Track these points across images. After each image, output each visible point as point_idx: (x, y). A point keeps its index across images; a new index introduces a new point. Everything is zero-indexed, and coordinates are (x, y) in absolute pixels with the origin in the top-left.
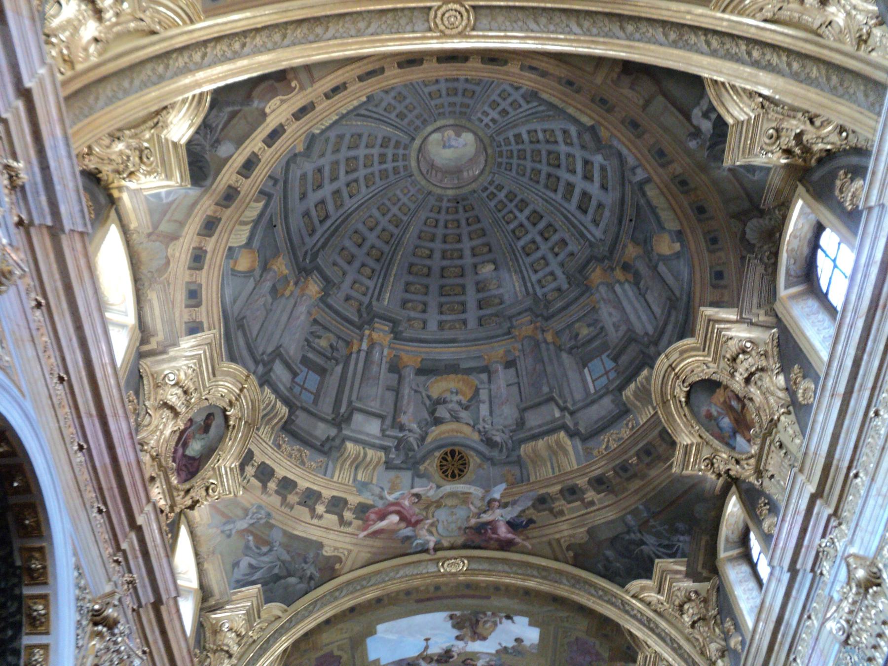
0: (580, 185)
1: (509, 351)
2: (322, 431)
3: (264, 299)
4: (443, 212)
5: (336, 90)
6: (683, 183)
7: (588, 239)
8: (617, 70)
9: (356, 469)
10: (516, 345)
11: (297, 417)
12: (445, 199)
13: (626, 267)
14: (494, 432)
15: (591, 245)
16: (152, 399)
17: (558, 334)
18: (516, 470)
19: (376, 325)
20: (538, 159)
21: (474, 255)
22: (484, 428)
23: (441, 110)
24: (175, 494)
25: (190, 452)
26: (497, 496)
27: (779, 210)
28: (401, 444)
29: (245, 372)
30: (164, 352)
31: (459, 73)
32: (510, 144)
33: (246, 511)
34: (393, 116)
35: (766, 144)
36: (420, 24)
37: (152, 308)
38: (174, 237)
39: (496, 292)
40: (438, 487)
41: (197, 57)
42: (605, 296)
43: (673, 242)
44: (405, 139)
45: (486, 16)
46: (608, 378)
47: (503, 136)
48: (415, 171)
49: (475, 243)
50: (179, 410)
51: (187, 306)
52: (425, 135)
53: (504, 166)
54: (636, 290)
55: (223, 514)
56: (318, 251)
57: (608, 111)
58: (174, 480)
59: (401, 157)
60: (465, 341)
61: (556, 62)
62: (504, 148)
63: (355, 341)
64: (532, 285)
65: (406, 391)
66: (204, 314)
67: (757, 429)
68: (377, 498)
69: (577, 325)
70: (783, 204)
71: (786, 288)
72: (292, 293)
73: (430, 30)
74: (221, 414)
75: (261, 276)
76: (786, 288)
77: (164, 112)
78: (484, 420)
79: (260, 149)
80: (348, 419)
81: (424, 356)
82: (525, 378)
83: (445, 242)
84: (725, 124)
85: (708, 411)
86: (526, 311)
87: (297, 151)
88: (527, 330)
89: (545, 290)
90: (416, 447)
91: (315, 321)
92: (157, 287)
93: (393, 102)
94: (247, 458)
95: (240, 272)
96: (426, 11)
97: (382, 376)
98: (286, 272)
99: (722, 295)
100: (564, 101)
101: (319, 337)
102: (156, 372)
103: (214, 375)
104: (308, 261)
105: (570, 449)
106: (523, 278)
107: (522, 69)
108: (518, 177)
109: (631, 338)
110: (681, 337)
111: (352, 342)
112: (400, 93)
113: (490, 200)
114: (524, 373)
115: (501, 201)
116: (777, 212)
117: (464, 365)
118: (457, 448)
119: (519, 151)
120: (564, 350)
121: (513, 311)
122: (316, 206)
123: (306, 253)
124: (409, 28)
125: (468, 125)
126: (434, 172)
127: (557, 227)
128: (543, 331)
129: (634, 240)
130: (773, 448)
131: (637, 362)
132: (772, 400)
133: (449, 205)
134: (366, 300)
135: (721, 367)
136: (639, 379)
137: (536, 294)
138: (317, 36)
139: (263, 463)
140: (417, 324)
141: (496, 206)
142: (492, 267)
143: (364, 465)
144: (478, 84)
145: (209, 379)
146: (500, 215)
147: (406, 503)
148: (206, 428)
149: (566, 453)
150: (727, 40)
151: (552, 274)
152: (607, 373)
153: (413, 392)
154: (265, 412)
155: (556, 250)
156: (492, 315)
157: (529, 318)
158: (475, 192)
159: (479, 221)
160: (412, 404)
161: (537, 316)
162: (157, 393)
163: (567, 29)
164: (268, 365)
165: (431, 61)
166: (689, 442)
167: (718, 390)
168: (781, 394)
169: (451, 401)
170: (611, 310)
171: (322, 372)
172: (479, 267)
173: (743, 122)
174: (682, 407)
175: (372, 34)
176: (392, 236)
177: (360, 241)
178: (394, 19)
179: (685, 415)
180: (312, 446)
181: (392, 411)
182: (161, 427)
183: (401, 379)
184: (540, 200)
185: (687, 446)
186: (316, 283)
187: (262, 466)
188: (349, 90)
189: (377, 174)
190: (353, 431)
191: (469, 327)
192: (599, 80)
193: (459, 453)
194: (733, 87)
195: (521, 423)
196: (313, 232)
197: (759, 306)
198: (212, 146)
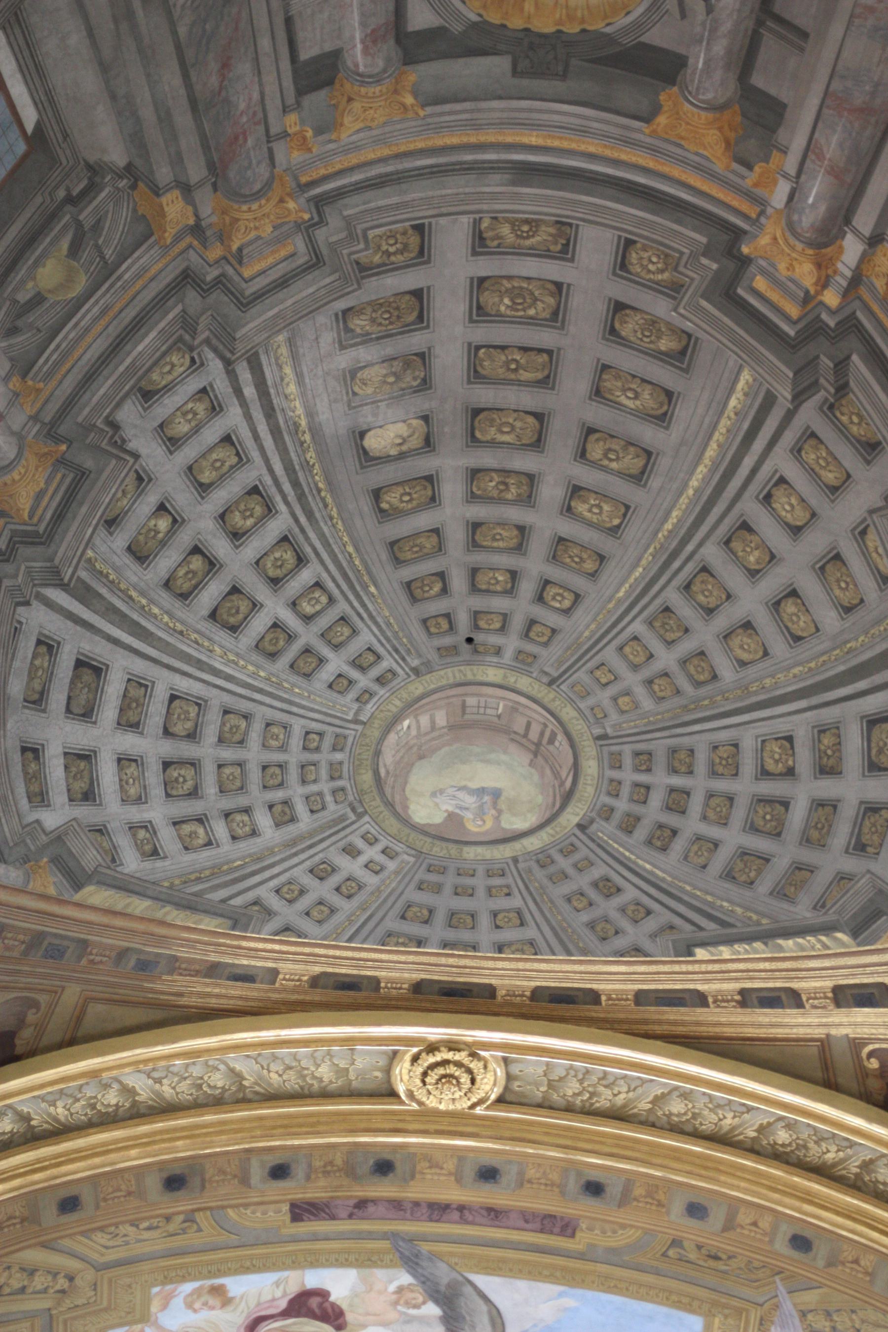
1: (319, 131)
7: (63, 586)
19: (794, 311)
20: (227, 771)
23: (497, 881)
31: (443, 960)
39: (364, 354)
44: (604, 830)
47: (325, 816)
48: (589, 750)
49: (424, 520)
52: (548, 830)
57: (40, 936)
59: (625, 790)
60: (482, 169)
61: (184, 1001)
64: (238, 392)
69: (81, 283)
82: (262, 22)
83: (522, 529)
86: (259, 296)
93: (625, 924)
96: (509, 1097)
97: (813, 102)
100: (162, 923)
106: (270, 412)
107: (275, 972)
108: (284, 717)
114: (265, 43)
115: (336, 647)
117: (499, 65)
119: (281, 785)
126: (534, 735)
127: (165, 597)
128: (197, 230)
133: (494, 640)
137: (228, 364)
141: (355, 632)
142: (372, 442)
144: (390, 935)
146: (342, 607)
151: (173, 443)
155: (163, 524)
157: (247, 273)
158: (416, 671)
161: (220, 282)
172: (416, 442)
177: (790, 607)
184: (217, 665)
188: (738, 986)
189: (701, 767)
191: (465, 220)
192: (72, 995)
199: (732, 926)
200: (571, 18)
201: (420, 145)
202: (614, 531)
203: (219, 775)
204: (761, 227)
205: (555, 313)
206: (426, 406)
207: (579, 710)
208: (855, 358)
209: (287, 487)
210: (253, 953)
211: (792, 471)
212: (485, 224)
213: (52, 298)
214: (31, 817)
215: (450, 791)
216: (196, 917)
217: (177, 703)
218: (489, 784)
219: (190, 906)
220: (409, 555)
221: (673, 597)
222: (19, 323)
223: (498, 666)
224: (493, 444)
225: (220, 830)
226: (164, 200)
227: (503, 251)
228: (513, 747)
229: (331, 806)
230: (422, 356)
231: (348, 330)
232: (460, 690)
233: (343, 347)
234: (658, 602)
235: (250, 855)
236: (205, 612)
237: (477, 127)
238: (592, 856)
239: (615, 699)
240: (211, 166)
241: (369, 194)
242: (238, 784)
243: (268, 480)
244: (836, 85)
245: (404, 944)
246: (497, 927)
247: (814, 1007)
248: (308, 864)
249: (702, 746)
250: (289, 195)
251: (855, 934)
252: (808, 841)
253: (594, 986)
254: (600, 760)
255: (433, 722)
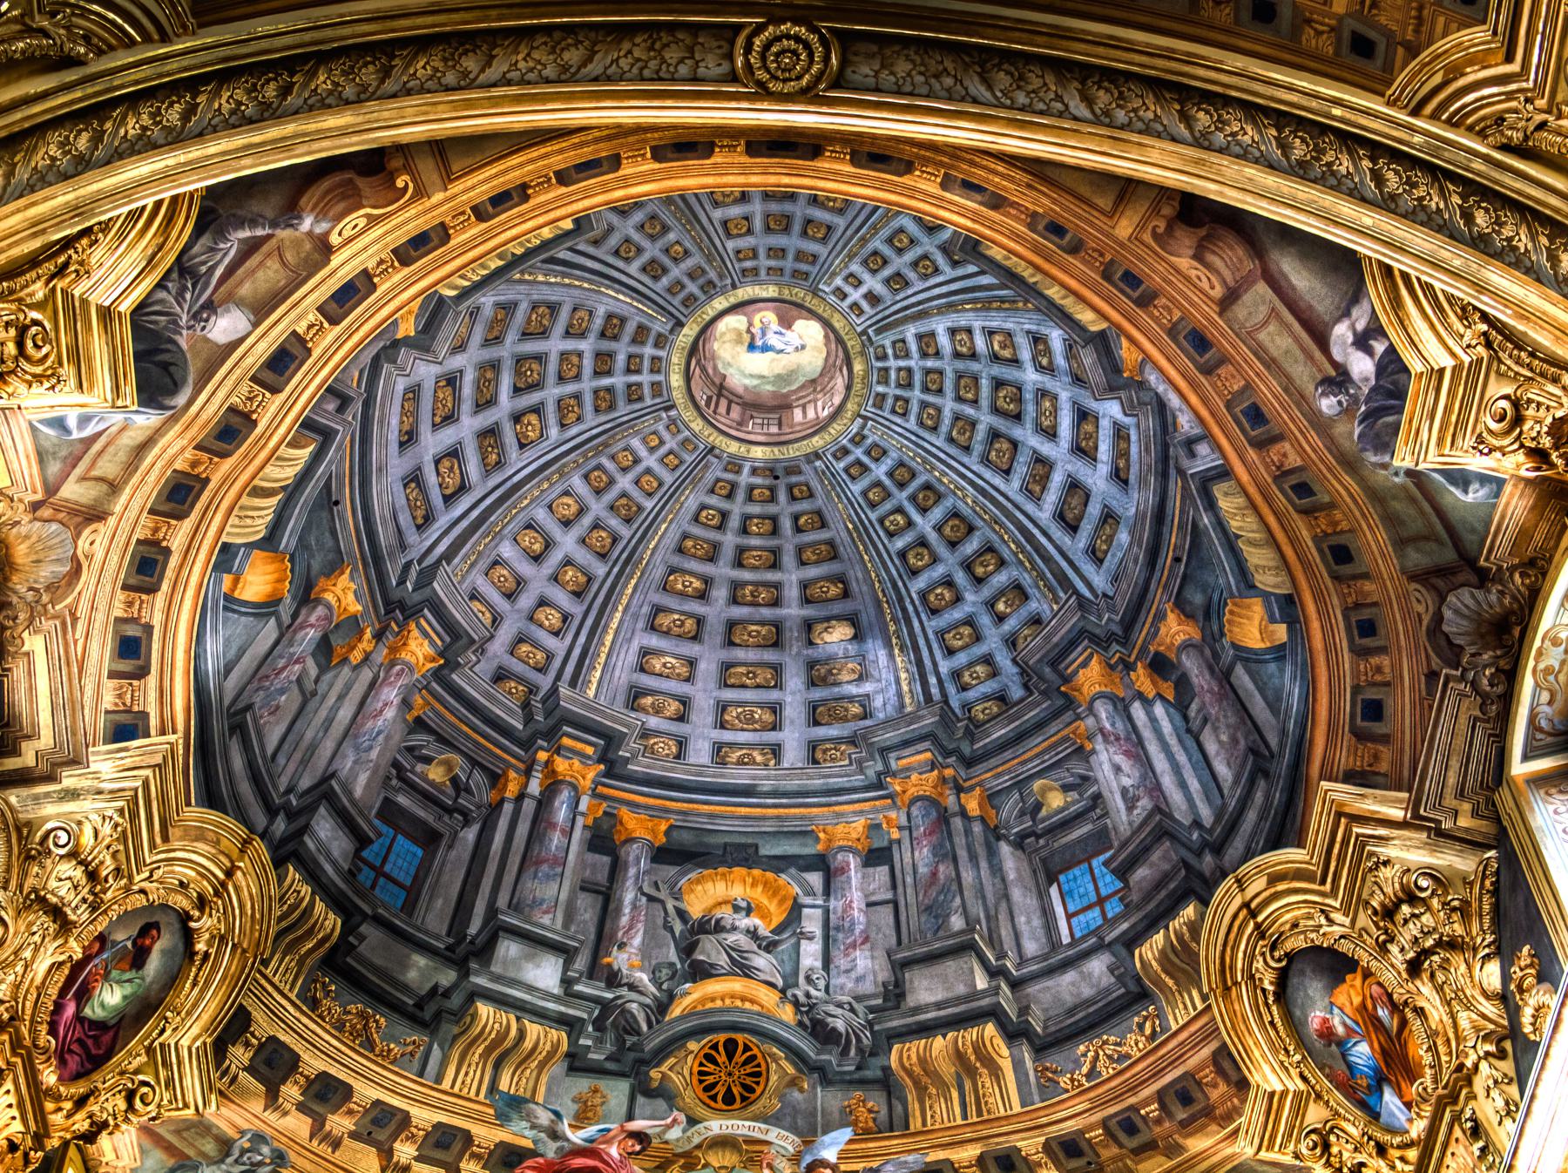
0: (1065, 466)
1: (878, 826)
2: (419, 971)
3: (297, 667)
4: (741, 495)
5: (501, 200)
6: (1303, 489)
7: (1076, 592)
8: (1167, 211)
9: (497, 1066)
10: (893, 814)
11: (362, 938)
12: (746, 470)
13: (1160, 666)
14: (831, 1009)
15: (1082, 604)
16: (13, 884)
17: (992, 798)
18: (877, 1101)
19: (566, 741)
20: (970, 396)
21: (807, 600)
22: (808, 995)
23: (748, 264)
24: (49, 1106)
25: (93, 1011)
26: (830, 1155)
27: (1522, 575)
28: (609, 1017)
29: (242, 832)
30: (51, 778)
32: (907, 356)
33: (225, 1145)
34: (633, 268)
35: (1490, 432)
36: (712, 66)
37: (31, 673)
38: (94, 515)
39: (853, 690)
40: (692, 1121)
41: (173, 115)
42: (1108, 726)
43: (1272, 620)
44: (660, 325)
45: (872, 56)
46: (1103, 913)
48: (679, 396)
49: (812, 572)
50: (73, 917)
51: (113, 675)
52: (708, 318)
53: (890, 401)
54: (1178, 718)
55: (169, 1148)
56: (438, 562)
58: (49, 1077)
59: (646, 364)
60: (775, 793)
61: (1026, 178)
62: (892, 363)
63: (512, 774)
64: (940, 681)
65: (629, 897)
66: (152, 696)
67: (1428, 1079)
68: (543, 1135)
69: (1037, 785)
70: (1532, 563)
71: (1526, 757)
72: (367, 657)
73: (733, 78)
74: (177, 926)
75: (295, 616)
76: (1526, 757)
77: (85, 241)
78: (809, 979)
79: (310, 326)
80: (484, 951)
81: (674, 820)
82: (910, 891)
83: (739, 563)
84: (1406, 370)
85: (1325, 1020)
86: (922, 738)
87: (400, 335)
88: (922, 783)
89: (971, 695)
90: (645, 1027)
91: (420, 724)
92: (48, 625)
93: (636, 237)
94: (234, 1027)
95: (245, 603)
97: (571, 857)
98: (356, 608)
99: (1376, 757)
100: (1037, 268)
101: (428, 760)
102: (29, 824)
103: (166, 839)
104: (409, 586)
105: (1006, 1065)
106: (920, 663)
108: (921, 432)
109: (1161, 827)
110: (1275, 843)
111: (505, 773)
112: (653, 217)
113: (853, 478)
114: (909, 880)
116: (1517, 576)
118: (740, 1038)
119: (928, 372)
120: (1006, 838)
121: (890, 736)
122: (437, 462)
123: (407, 566)
124: (683, 70)
125: (810, 301)
126: (723, 403)
127: (1006, 554)
128: (959, 789)
129: (1181, 604)
130: (1457, 1133)
131: (1172, 886)
132: (1464, 1019)
133: (758, 481)
134: (545, 682)
135: (1359, 924)
136: (1175, 924)
137: (945, 700)
138: (465, 74)
139: (273, 1039)
140: (667, 748)
141: (864, 493)
143: (515, 1059)
144: (841, 212)
145: (153, 846)
146: (873, 516)
147: (614, 1151)
148: (138, 958)
149: (996, 1072)
150: (1419, 176)
151: (988, 660)
152: (1101, 901)
153: (644, 899)
154: (284, 924)
155: (1001, 607)
156: (837, 741)
157: (928, 755)
158: (817, 456)
159: (824, 525)
160: (640, 926)
161: (947, 753)
162: (24, 874)
163: (1059, 106)
164: (300, 817)
165: (732, 148)
166: (1279, 1088)
167: (1349, 977)
168: (1490, 1009)
169: (734, 928)
170: (1120, 759)
171: (430, 839)
172: (819, 628)
173: (1442, 371)
174: (1267, 1004)
175: (596, 80)
176: (615, 540)
177: (537, 547)
178: (651, 48)
179: (1272, 1023)
180: (395, 1007)
181: (592, 937)
182: (27, 954)
183: (616, 869)
185: (1272, 1094)
186: (426, 635)
187: (270, 1048)
188: (532, 202)
189: (588, 400)
190: (497, 978)
192: (1124, 228)
193: (747, 1048)
194: (1428, 288)
195: (895, 994)
196: (429, 519)
197: (1461, 794)
198: (195, 316)
199: (544, 261)
200: (724, 875)
201: (815, 810)
202: (673, 570)
203: (977, 394)
204: (593, 782)
205: (724, 709)
206: (810, 652)
207: (688, 428)
208: (520, 727)
209: (910, 608)
210: (962, 211)
211: (551, 642)
212: (772, 762)
213: (1056, 784)
214: (1128, 420)
215: (790, 349)
216: (1007, 263)
217: (1005, 467)
218: (757, 356)
219: (1011, 277)
220: (823, 547)
221: (625, 532)
222: (1078, 781)
223: (754, 460)
224: (762, 623)
225: (980, 343)
226: (978, 813)
227: (761, 746)
228: (740, 391)
229: (887, 343)
230: (814, 684)
231: (863, 706)
232: (783, 438)
233: (868, 695)
234: (635, 526)
235: (958, 311)
236: (978, 533)
237: (778, 817)
238: (669, 297)
239: (662, 442)
240: (947, 823)
241: (848, 785)
242: (963, 382)
243: (923, 616)
244: (559, 870)
245: (828, 199)
246: (747, 218)
247: (463, 213)
248: (910, 292)
249: (591, 419)
250: (897, 794)
251: (441, 300)
252: (493, 366)
253: (657, 166)
254: (669, 388)
255: (804, 412)
